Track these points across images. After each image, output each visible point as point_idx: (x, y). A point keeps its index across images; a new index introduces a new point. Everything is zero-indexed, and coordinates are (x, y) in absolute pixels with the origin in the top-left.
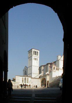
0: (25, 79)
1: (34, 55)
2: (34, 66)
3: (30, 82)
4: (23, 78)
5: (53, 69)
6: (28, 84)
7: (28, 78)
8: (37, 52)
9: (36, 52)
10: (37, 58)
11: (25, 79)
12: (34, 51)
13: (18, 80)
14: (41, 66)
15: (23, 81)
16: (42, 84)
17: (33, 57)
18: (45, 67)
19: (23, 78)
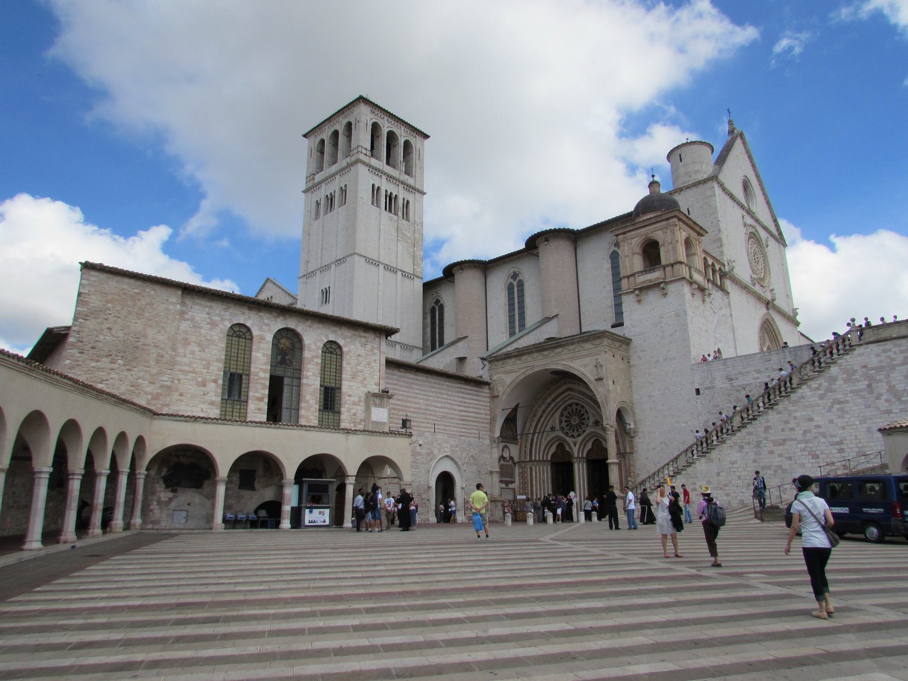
0: (288, 349)
1: (374, 162)
2: (376, 263)
3: (380, 414)
4: (240, 333)
5: (682, 256)
6: (351, 453)
7: (332, 349)
8: (407, 144)
9: (391, 136)
10: (402, 194)
11: (288, 349)
12: (375, 128)
13: (131, 352)
14: (450, 272)
15: (235, 384)
16: (514, 451)
17: (363, 180)
18: (498, 282)
19: (240, 333)
